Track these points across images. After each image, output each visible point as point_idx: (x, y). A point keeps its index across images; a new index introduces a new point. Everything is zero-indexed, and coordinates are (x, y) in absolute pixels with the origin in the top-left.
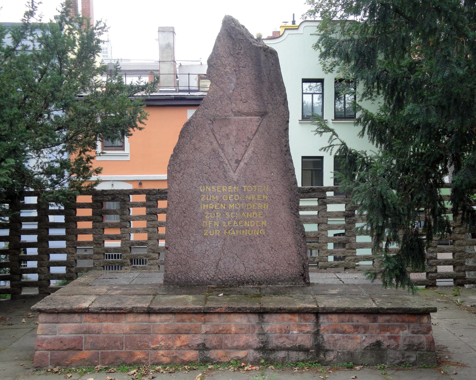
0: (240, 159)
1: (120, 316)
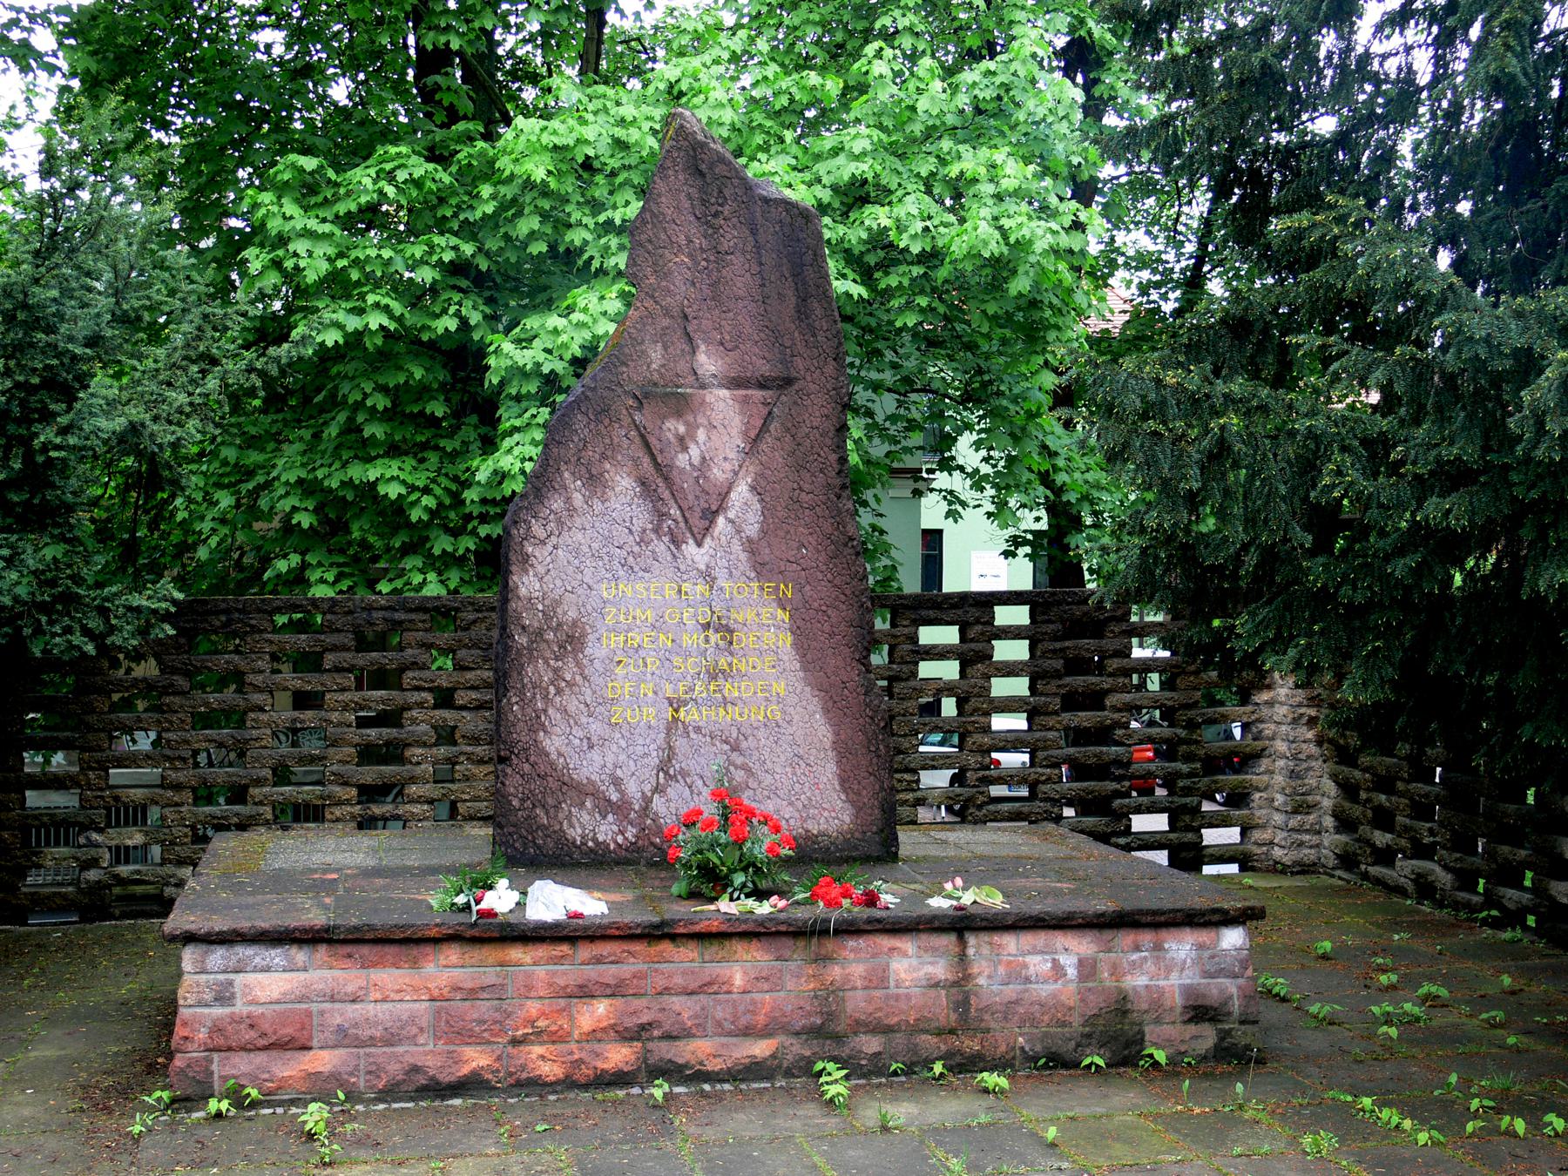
0: (714, 508)
1: (415, 951)
